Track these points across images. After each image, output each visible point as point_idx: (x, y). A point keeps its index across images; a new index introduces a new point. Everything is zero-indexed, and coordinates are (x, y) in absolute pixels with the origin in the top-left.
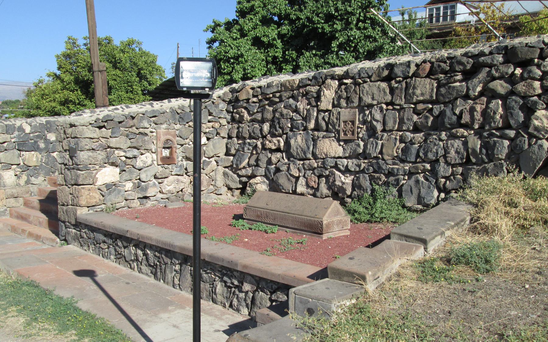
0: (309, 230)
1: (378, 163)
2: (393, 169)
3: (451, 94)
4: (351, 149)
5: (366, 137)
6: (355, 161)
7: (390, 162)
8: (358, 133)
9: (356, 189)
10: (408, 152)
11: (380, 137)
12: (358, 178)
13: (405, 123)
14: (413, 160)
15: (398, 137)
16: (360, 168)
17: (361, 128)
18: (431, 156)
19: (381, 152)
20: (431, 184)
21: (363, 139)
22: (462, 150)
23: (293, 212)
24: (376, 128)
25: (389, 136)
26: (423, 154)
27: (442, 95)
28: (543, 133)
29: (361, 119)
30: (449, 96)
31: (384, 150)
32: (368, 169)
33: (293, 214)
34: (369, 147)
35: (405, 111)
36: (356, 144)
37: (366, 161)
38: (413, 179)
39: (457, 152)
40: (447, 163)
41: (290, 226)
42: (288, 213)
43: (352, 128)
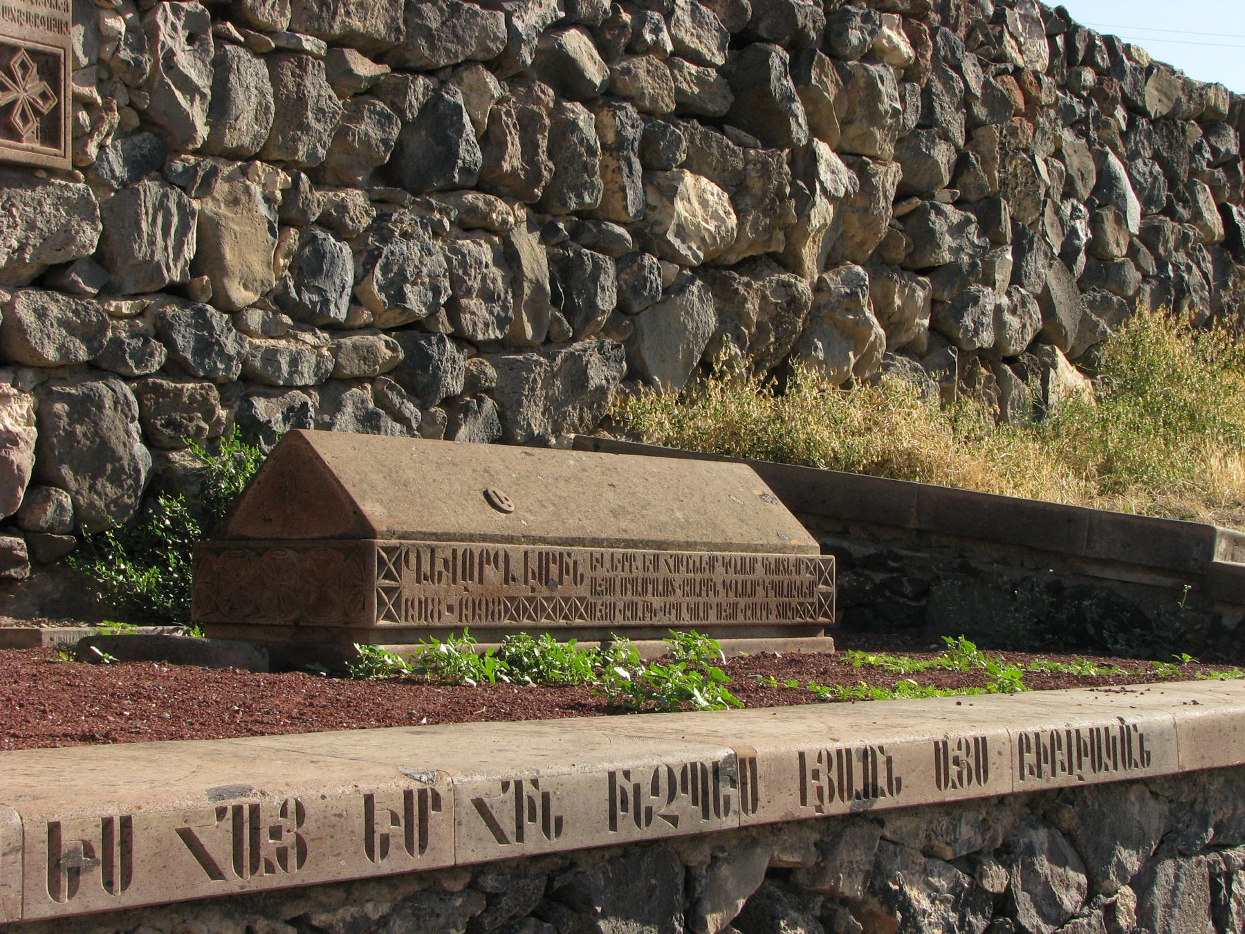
0: (773, 619)
1: (202, 321)
2: (271, 356)
3: (460, 40)
4: (31, 226)
5: (117, 165)
6: (57, 306)
7: (255, 319)
8: (81, 137)
9: (66, 471)
10: (329, 275)
11: (201, 173)
12: (85, 408)
13: (306, 128)
14: (342, 316)
15: (279, 195)
16: (91, 350)
17: (88, 104)
18: (415, 300)
19: (195, 267)
20: (410, 428)
21: (105, 172)
22: (500, 280)
23: (681, 537)
24: (192, 127)
25: (229, 179)
26: (381, 289)
27: (429, 36)
28: (694, 247)
29: (84, 61)
30: (452, 47)
31: (229, 255)
32: (142, 357)
33: (690, 545)
34: (144, 226)
35: (302, 67)
36: (61, 201)
37: (126, 307)
38: (349, 409)
39: (488, 296)
40: (462, 340)
41: (686, 619)
42: (660, 545)
43: (44, 96)
